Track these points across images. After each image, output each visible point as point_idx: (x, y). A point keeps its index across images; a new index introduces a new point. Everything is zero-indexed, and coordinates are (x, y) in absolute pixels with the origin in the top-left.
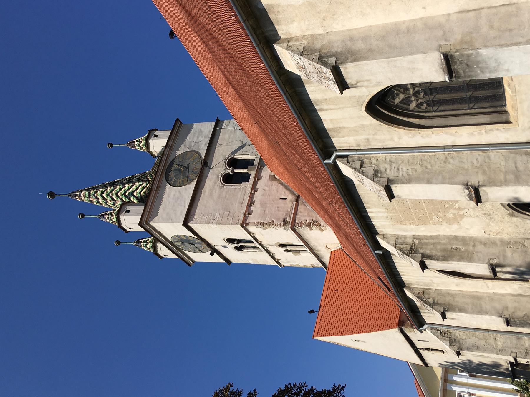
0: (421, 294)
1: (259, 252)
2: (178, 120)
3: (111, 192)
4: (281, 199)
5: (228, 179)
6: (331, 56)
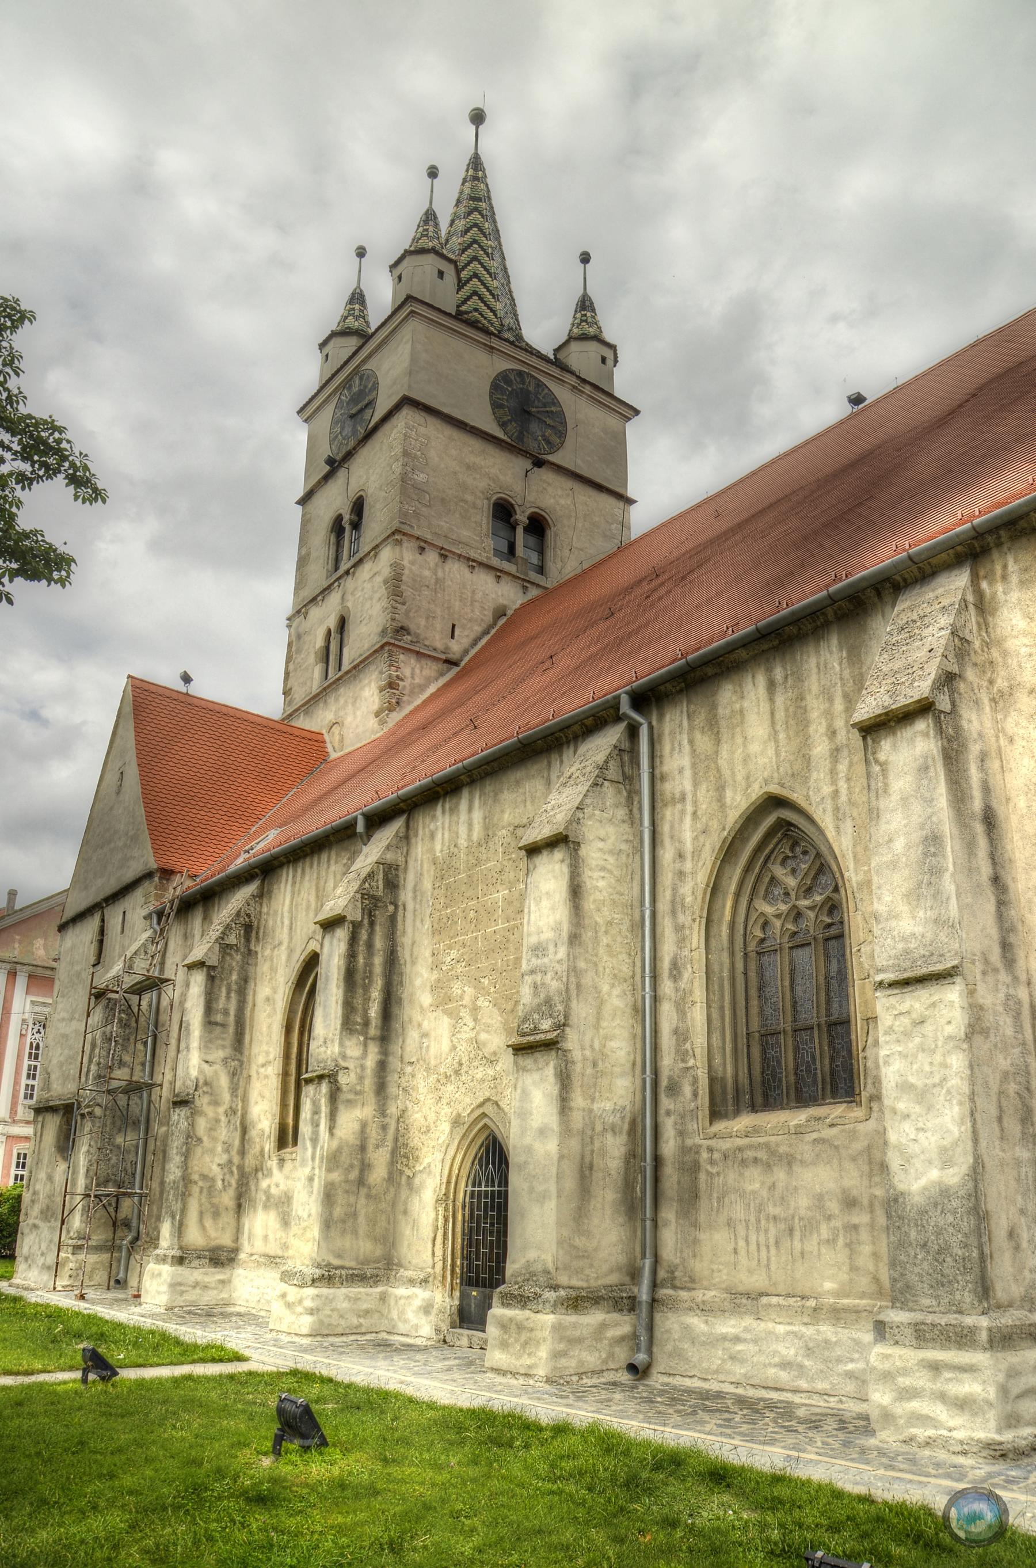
0: (247, 920)
1: (328, 571)
4: (454, 626)
6: (953, 704)
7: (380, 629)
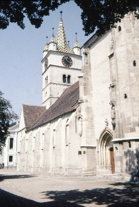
5: (64, 76)
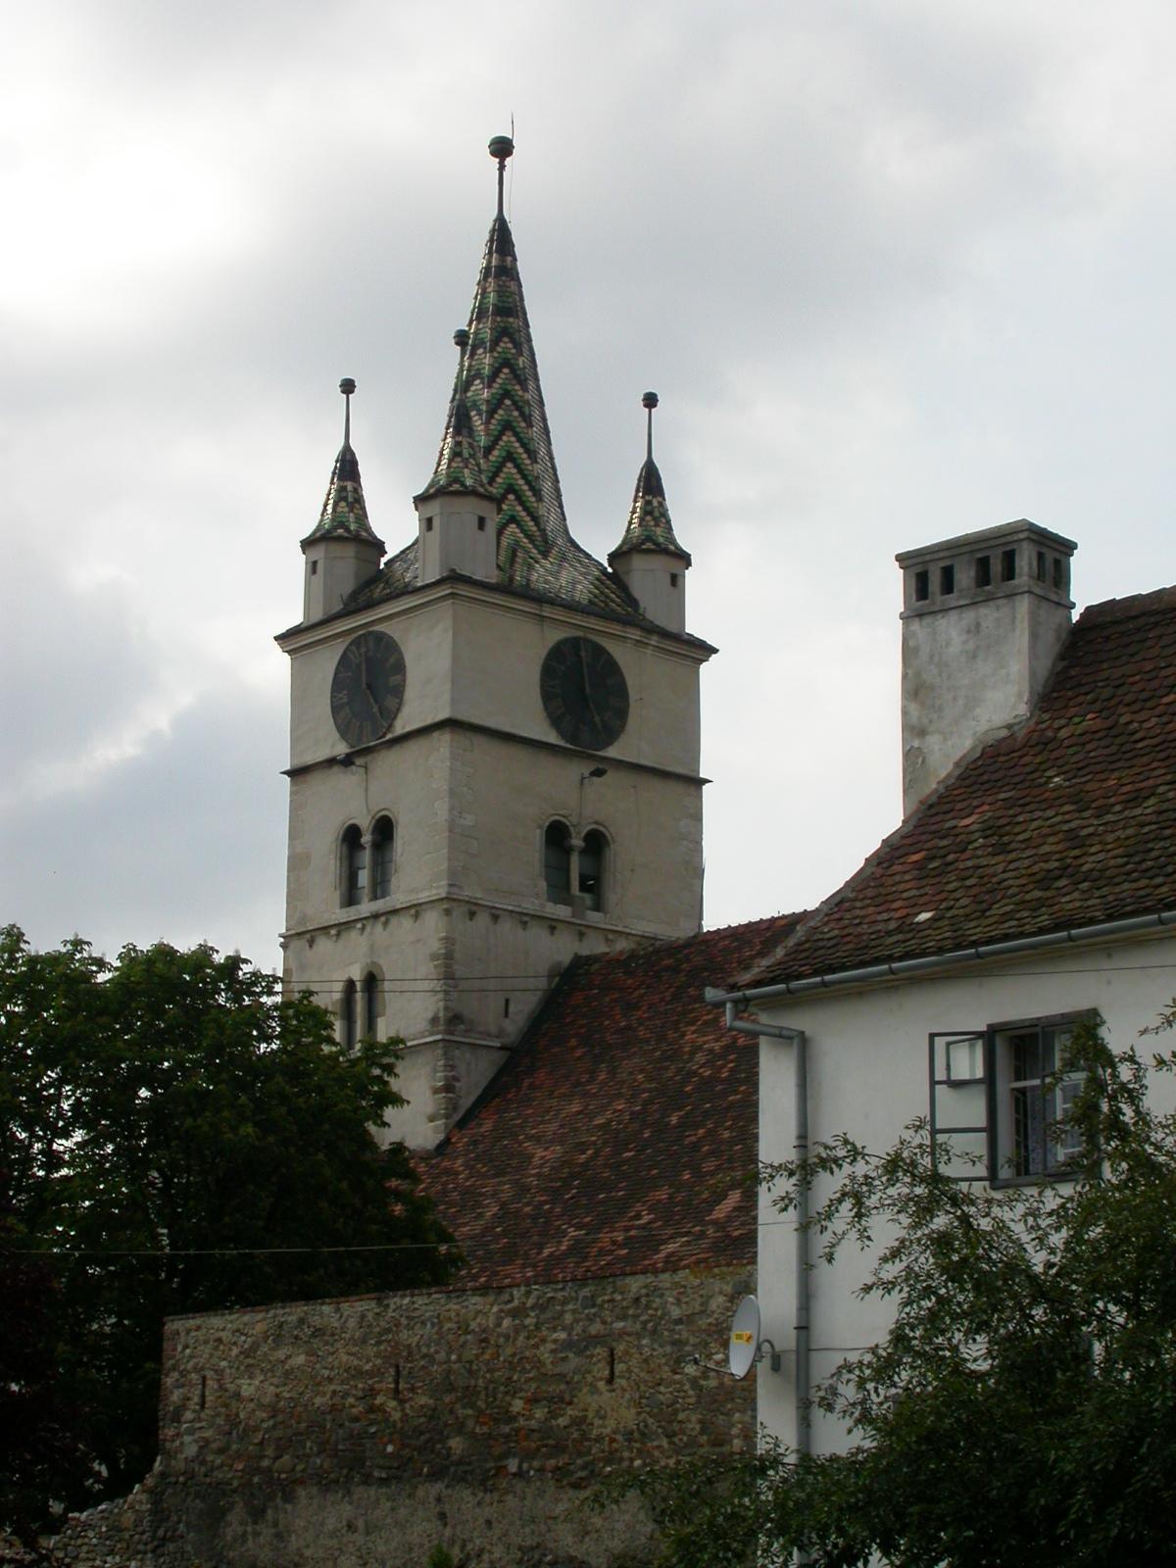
2: (715, 651)
3: (515, 403)
5: (556, 835)
7: (430, 1015)
